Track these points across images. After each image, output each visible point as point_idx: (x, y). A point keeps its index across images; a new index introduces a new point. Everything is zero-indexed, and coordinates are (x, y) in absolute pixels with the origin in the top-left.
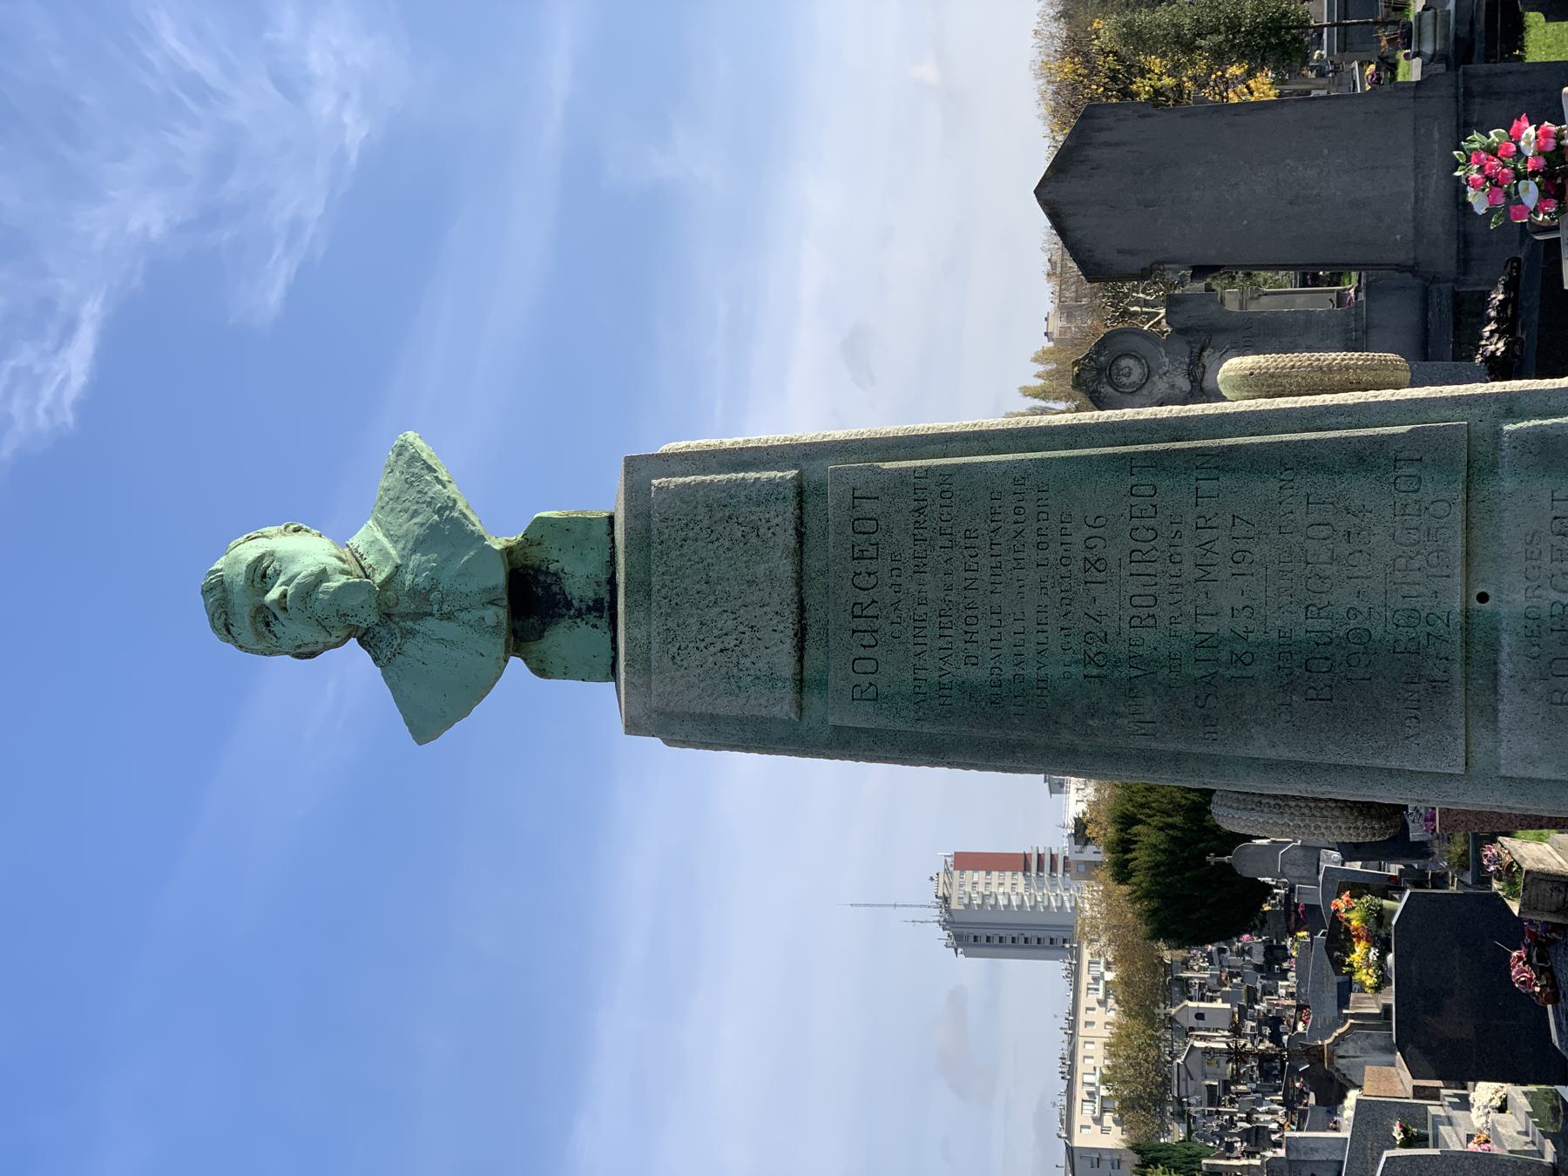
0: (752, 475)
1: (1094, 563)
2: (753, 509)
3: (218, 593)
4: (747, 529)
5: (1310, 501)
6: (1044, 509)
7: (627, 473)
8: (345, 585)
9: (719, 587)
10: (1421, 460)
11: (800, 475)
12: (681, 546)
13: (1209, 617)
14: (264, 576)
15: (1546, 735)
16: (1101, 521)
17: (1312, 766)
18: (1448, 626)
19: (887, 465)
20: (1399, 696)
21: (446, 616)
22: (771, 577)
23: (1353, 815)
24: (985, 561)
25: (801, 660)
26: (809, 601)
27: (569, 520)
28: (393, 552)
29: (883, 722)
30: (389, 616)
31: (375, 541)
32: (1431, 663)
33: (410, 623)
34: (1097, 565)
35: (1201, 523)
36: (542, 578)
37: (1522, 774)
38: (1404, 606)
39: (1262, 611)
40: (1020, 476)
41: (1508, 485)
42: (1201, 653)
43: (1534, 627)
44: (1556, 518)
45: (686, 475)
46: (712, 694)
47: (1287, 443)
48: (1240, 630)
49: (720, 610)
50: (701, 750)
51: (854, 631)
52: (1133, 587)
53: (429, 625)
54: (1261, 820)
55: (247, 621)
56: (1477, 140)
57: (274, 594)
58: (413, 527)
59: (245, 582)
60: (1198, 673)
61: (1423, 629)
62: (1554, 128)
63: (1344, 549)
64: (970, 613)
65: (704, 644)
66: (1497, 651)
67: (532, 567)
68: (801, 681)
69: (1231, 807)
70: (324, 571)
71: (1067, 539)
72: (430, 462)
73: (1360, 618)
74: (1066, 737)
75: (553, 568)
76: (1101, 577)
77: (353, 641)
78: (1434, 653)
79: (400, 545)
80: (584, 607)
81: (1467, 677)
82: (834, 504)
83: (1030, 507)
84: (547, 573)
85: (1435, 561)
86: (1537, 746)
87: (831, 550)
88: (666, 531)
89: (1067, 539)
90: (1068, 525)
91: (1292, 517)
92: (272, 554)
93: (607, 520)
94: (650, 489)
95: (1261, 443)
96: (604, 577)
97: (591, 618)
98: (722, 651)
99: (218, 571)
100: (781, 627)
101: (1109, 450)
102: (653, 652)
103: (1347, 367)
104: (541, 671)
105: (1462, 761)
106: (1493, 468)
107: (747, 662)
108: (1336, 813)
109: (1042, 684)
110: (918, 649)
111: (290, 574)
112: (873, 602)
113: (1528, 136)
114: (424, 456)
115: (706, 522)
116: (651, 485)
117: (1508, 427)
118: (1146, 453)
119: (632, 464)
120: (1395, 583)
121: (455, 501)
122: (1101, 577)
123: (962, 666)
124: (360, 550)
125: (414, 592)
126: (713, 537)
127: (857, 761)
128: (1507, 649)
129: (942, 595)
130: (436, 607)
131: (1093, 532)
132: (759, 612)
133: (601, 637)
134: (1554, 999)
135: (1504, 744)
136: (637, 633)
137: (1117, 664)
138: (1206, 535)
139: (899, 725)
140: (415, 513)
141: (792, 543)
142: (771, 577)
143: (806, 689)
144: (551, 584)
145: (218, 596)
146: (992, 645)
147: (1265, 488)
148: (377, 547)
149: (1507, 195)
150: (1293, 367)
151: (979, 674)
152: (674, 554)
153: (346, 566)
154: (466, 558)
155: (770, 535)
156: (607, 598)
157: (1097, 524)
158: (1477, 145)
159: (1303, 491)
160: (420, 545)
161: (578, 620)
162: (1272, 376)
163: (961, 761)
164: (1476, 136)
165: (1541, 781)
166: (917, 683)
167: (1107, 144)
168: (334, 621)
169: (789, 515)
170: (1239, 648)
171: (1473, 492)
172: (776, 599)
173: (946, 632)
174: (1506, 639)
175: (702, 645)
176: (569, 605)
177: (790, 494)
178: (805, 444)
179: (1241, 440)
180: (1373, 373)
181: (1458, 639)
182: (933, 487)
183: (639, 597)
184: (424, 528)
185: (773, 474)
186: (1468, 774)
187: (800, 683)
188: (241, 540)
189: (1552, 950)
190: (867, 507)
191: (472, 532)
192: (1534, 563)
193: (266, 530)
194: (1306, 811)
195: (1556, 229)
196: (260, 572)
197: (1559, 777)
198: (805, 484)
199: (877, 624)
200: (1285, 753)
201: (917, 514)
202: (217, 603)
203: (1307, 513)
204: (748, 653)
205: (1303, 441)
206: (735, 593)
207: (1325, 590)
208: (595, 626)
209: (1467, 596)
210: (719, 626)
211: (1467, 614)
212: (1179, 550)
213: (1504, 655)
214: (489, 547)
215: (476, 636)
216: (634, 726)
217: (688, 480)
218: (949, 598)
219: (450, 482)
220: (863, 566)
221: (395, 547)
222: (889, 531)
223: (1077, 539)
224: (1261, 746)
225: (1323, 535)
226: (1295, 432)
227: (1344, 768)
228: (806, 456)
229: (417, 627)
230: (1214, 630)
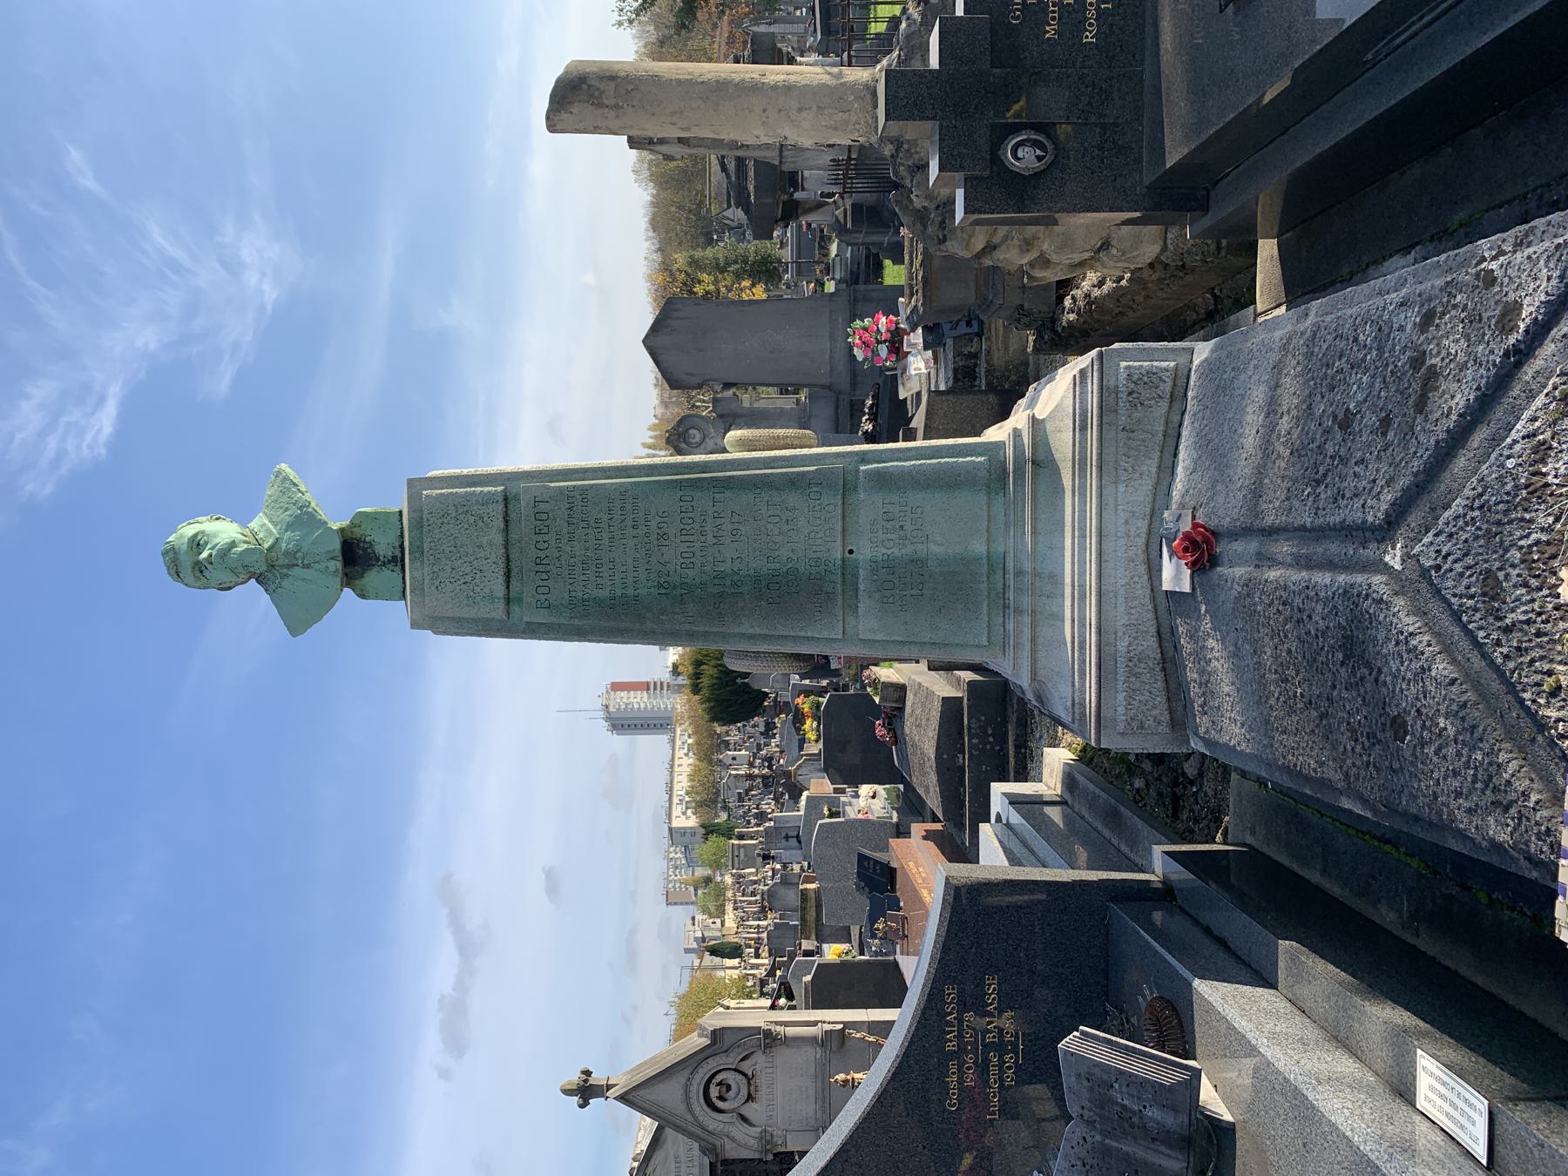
0: (479, 489)
1: (663, 536)
3: (171, 555)
11: (506, 489)
14: (198, 544)
16: (666, 514)
19: (553, 485)
22: (491, 543)
25: (508, 587)
27: (376, 513)
28: (274, 531)
29: (553, 619)
31: (264, 525)
33: (285, 571)
35: (716, 515)
36: (362, 545)
40: (623, 491)
41: (862, 496)
42: (716, 581)
43: (875, 567)
45: (442, 489)
47: (757, 475)
52: (683, 547)
55: (190, 570)
57: (205, 555)
58: (285, 517)
60: (715, 591)
62: (894, 319)
63: (786, 528)
66: (858, 578)
70: (234, 542)
71: (648, 523)
72: (295, 481)
74: (649, 625)
75: (368, 539)
76: (665, 543)
77: (253, 580)
81: (843, 591)
82: (524, 504)
83: (629, 507)
84: (365, 542)
89: (648, 523)
92: (203, 532)
96: (397, 544)
101: (669, 477)
103: (787, 437)
104: (363, 596)
107: (479, 589)
110: (571, 581)
114: (291, 477)
115: (454, 515)
117: (862, 468)
119: (411, 483)
122: (665, 543)
125: (287, 553)
126: (458, 522)
131: (662, 520)
132: (485, 562)
133: (397, 576)
134: (896, 744)
136: (418, 575)
137: (675, 587)
138: (719, 521)
139: (562, 621)
141: (502, 526)
142: (491, 543)
147: (747, 498)
149: (873, 351)
151: (603, 594)
152: (436, 531)
156: (399, 555)
159: (766, 499)
160: (289, 527)
164: (858, 321)
165: (879, 641)
167: (677, 318)
168: (241, 569)
170: (735, 578)
174: (862, 572)
175: (453, 580)
176: (378, 559)
177: (500, 499)
183: (417, 555)
185: (490, 489)
186: (843, 640)
187: (508, 600)
189: (894, 720)
190: (543, 506)
193: (200, 519)
195: (896, 369)
199: (549, 568)
200: (758, 631)
208: (393, 571)
209: (844, 551)
211: (843, 560)
213: (860, 580)
216: (415, 625)
220: (540, 538)
222: (555, 519)
223: (653, 524)
224: (746, 629)
227: (786, 637)
228: (509, 479)
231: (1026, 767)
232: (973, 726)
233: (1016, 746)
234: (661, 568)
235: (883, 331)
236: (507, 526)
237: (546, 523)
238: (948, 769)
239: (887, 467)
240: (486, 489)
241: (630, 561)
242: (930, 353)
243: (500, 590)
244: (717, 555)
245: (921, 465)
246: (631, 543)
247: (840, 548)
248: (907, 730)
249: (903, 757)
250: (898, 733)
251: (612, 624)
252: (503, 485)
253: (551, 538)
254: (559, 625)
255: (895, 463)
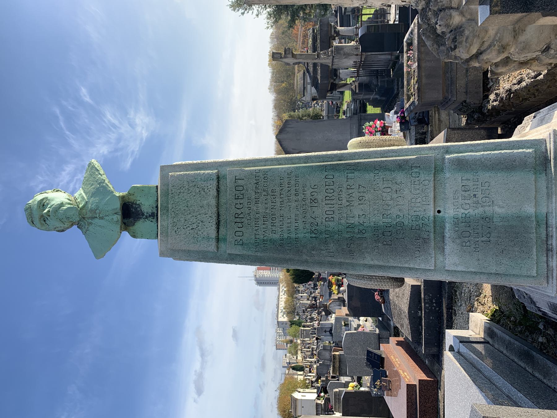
0: (203, 172)
1: (313, 200)
2: (202, 183)
3: (29, 211)
4: (200, 189)
5: (384, 180)
6: (297, 183)
7: (161, 171)
8: (69, 208)
9: (191, 208)
10: (419, 167)
11: (218, 172)
12: (179, 195)
13: (351, 218)
14: (44, 205)
15: (460, 256)
16: (316, 187)
17: (385, 266)
18: (429, 221)
19: (246, 169)
20: (413, 244)
21: (101, 218)
23: (392, 281)
24: (278, 200)
25: (218, 232)
26: (221, 213)
27: (143, 187)
28: (86, 197)
29: (245, 252)
30: (84, 218)
32: (424, 233)
33: (90, 221)
34: (315, 201)
35: (349, 187)
36: (134, 206)
37: (453, 269)
38: (415, 214)
39: (368, 216)
40: (289, 173)
41: (448, 175)
42: (349, 230)
43: (457, 221)
44: (463, 186)
45: (181, 172)
46: (189, 243)
47: (376, 161)
48: (361, 222)
49: (191, 216)
50: (186, 261)
51: (235, 223)
53: (96, 221)
54: (364, 283)
55: (38, 219)
56: (367, 124)
57: (45, 211)
58: (91, 189)
59: (37, 207)
60: (347, 236)
61: (421, 222)
62: (383, 122)
63: (395, 196)
64: (273, 216)
65: (186, 227)
66: (444, 229)
67: (131, 202)
68: (218, 239)
69: (354, 278)
70: (62, 203)
71: (305, 193)
72: (98, 168)
73: (400, 218)
74: (305, 257)
75: (138, 203)
76: (316, 205)
77: (75, 227)
78: (424, 230)
79: (88, 195)
80: (148, 215)
82: (229, 183)
83: (293, 182)
84: (136, 204)
85: (424, 200)
86: (458, 260)
87: (228, 196)
88: (174, 190)
89: (305, 193)
90: (305, 188)
91: (378, 185)
92: (47, 198)
93: (156, 187)
94: (168, 176)
95: (368, 162)
96: (155, 206)
97: (150, 219)
98: (192, 229)
99: (29, 203)
100: (211, 221)
101: (319, 164)
102: (169, 229)
103: (391, 140)
104: (134, 236)
105: (433, 265)
106: (442, 170)
107: (200, 233)
108: (388, 280)
109: (296, 240)
110: (257, 228)
111: (51, 204)
112: (242, 213)
113: (378, 123)
114: (96, 166)
115: (187, 187)
116: (169, 175)
117: (447, 156)
118: (331, 164)
119: (162, 168)
120: (412, 207)
121: (104, 180)
122: (316, 205)
123: (271, 234)
124: (77, 197)
125: (91, 210)
126: (189, 192)
127: (236, 264)
128: (447, 228)
129: (264, 211)
130: (98, 215)
132: (204, 216)
133: (153, 224)
134: (384, 303)
135: (447, 260)
138: (350, 191)
139: (250, 253)
140: (92, 185)
141: (215, 194)
142: (208, 205)
143: (220, 241)
144: (137, 208)
145: (29, 212)
146: (280, 227)
147: (370, 176)
148: (81, 196)
150: (374, 140)
151: (276, 236)
152: (176, 197)
153: (71, 202)
154: (107, 199)
155: (208, 191)
156: (156, 212)
157: (314, 188)
158: (367, 125)
159: (381, 177)
160: (93, 195)
161: (146, 220)
162: (367, 143)
163: (270, 265)
165: (459, 271)
166: (256, 239)
168: (65, 220)
169: (214, 184)
170: (361, 228)
171: (436, 178)
172: (210, 212)
173: (265, 223)
174: (448, 226)
175: (185, 227)
176: (143, 214)
177: (215, 178)
178: (220, 162)
179: (361, 161)
180: (398, 142)
181: (432, 225)
182: (261, 175)
183: (165, 211)
184: (95, 189)
185: (209, 171)
186: (435, 270)
187: (218, 240)
188: (38, 194)
189: (383, 292)
190: (240, 182)
191: (109, 190)
192: (456, 200)
193: (47, 191)
194: (379, 280)
196: (42, 204)
197: (465, 270)
198: (220, 175)
199: (243, 220)
200: (376, 263)
201: (256, 185)
202: (28, 214)
203: (383, 184)
204: (201, 229)
205: (382, 161)
206: (196, 210)
207: (389, 209)
208: (152, 221)
209: (435, 211)
210: (191, 221)
211: (435, 217)
212: (341, 196)
213: (447, 230)
214: (115, 195)
215: (110, 224)
216: (162, 254)
217: (181, 173)
218: (266, 212)
219: (104, 174)
220: (238, 201)
221: (86, 196)
222: (247, 190)
223: (308, 193)
224: (368, 261)
225: (388, 191)
226: (378, 158)
227: (395, 267)
228: (220, 166)
229: (92, 222)
230: (353, 222)
231: (452, 318)
232: (426, 298)
233: (447, 309)
234: (312, 220)
235: (378, 126)
236: (218, 194)
237: (242, 192)
238: (414, 318)
239: (464, 156)
240: (207, 172)
241: (293, 216)
242: (402, 133)
243: (213, 234)
244: (349, 213)
245: (488, 154)
246: (294, 204)
247: (432, 209)
248: (391, 298)
249: (388, 308)
250: (386, 298)
251: (281, 256)
252: (217, 169)
253: (245, 201)
254: (249, 256)
255: (470, 154)
